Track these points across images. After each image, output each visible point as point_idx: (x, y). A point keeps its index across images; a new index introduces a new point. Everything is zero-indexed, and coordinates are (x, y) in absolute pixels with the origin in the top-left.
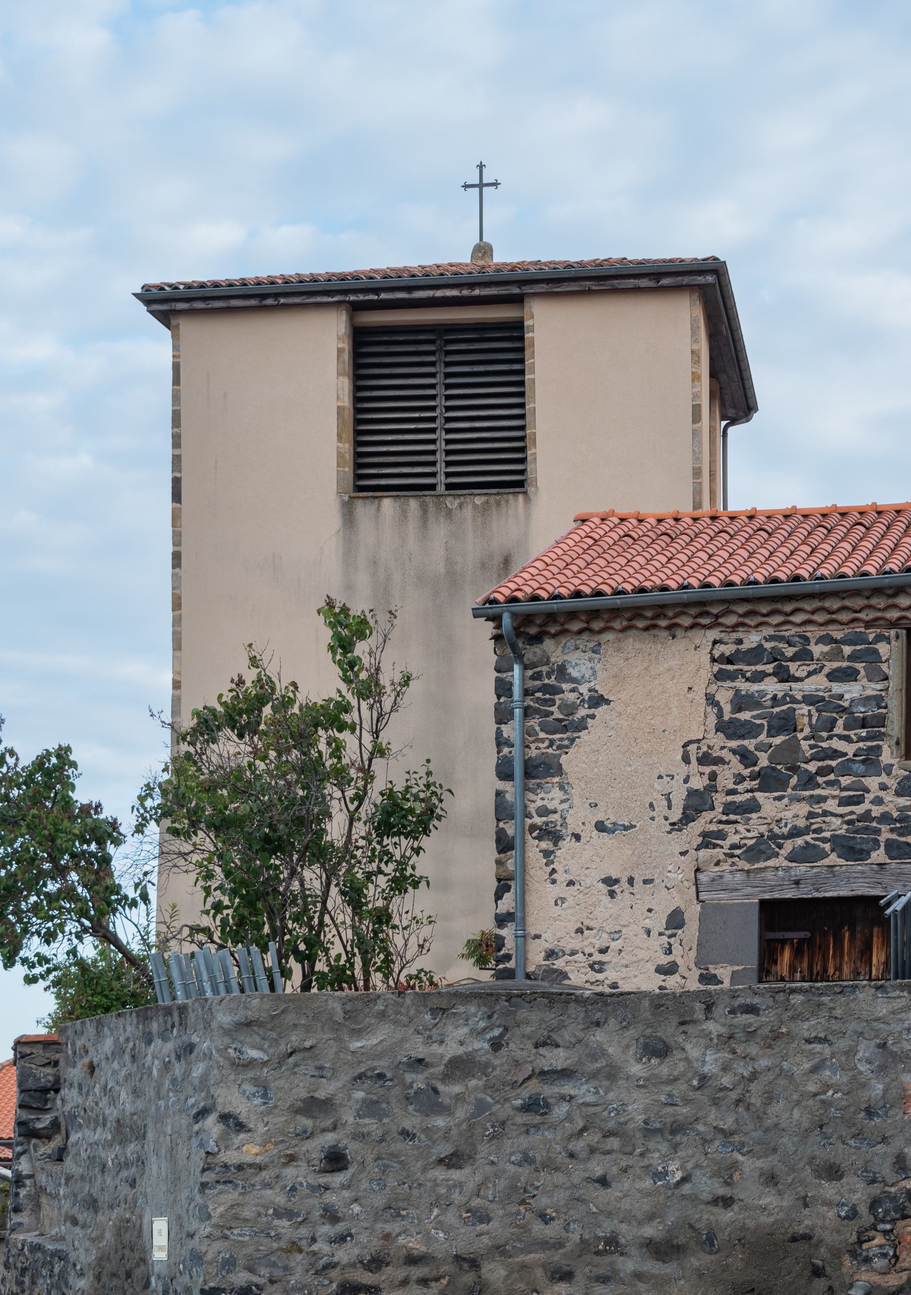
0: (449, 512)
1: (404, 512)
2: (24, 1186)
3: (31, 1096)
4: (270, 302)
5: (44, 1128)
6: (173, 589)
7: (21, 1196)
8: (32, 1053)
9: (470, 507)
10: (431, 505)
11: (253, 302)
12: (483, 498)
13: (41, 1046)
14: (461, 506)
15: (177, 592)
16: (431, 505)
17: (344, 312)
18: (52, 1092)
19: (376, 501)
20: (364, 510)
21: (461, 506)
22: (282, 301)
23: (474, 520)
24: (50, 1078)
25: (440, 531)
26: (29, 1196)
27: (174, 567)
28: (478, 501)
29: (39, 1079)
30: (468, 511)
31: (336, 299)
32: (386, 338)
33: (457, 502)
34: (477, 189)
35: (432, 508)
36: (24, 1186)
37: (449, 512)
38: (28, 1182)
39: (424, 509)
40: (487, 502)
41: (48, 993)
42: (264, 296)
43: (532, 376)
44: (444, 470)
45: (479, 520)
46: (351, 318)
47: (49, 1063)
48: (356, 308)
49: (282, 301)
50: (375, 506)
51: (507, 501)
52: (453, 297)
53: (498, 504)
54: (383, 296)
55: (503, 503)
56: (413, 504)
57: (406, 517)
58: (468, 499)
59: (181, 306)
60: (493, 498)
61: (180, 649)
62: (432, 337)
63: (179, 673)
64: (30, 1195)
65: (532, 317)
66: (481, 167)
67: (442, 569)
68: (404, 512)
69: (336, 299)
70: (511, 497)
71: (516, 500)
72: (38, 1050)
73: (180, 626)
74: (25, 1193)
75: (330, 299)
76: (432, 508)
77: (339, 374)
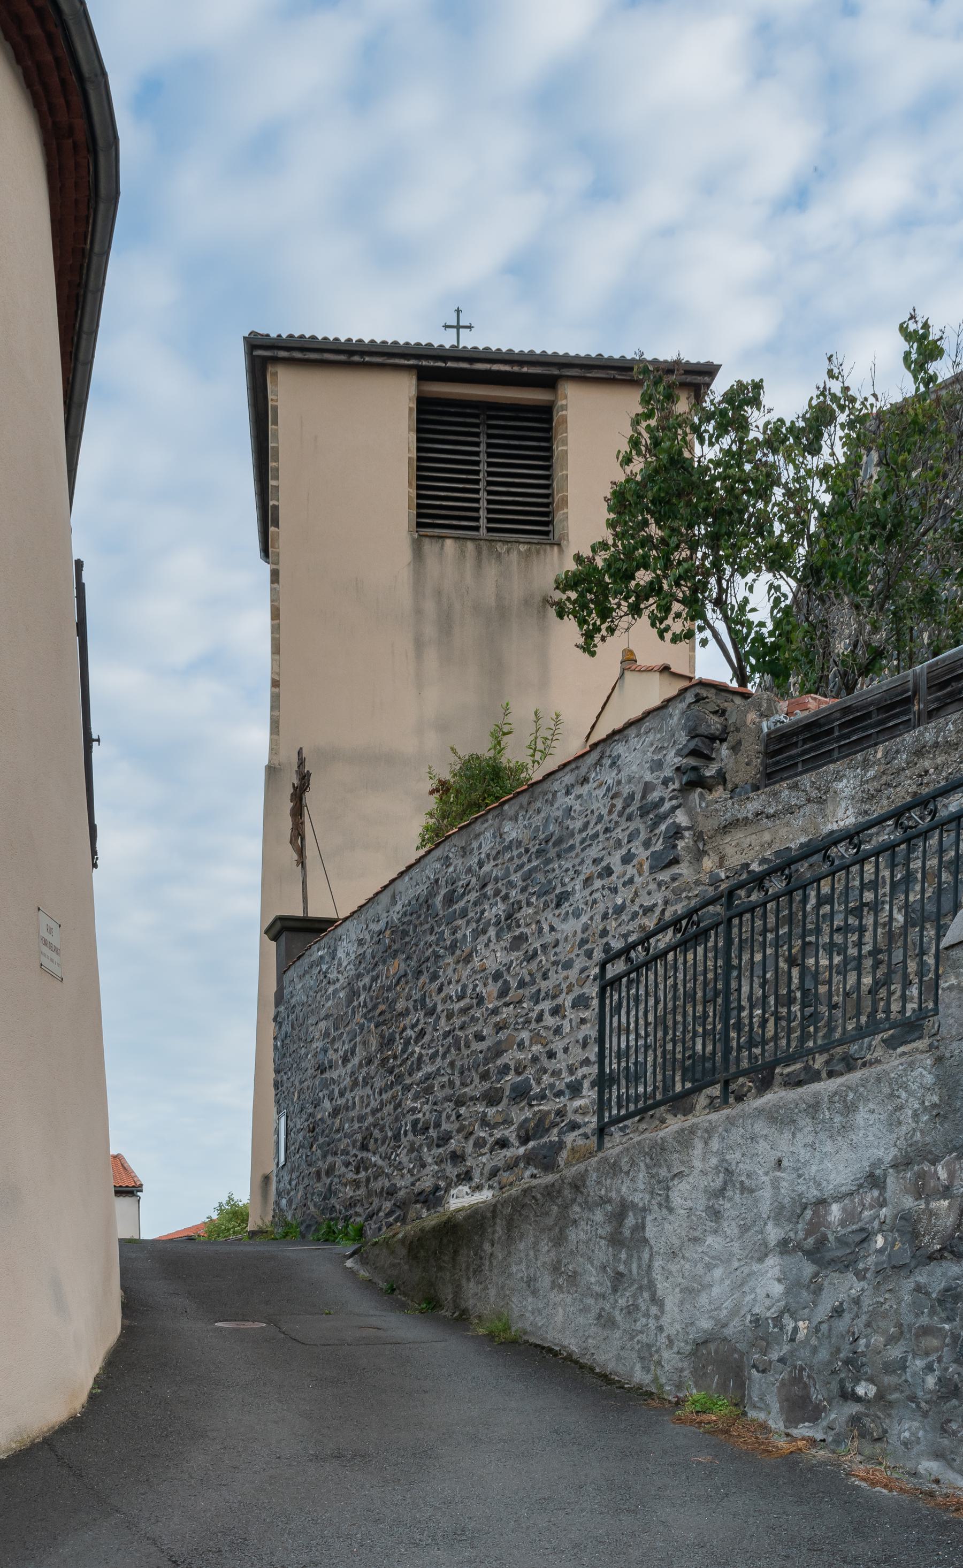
0: (499, 556)
1: (463, 552)
2: (682, 838)
3: (703, 742)
4: (356, 358)
5: (711, 777)
6: (272, 601)
7: (679, 848)
8: (707, 697)
9: (516, 552)
10: (484, 548)
11: (342, 357)
12: (526, 546)
13: (713, 691)
14: (508, 551)
15: (276, 604)
16: (484, 548)
17: (414, 377)
18: (718, 742)
19: (440, 541)
20: (429, 547)
21: (508, 551)
22: (367, 359)
23: (519, 564)
24: (719, 726)
25: (491, 571)
26: (687, 848)
27: (272, 582)
28: (522, 548)
29: (710, 726)
30: (514, 556)
31: (411, 362)
32: (440, 409)
33: (505, 547)
34: (461, 324)
35: (485, 552)
36: (682, 838)
37: (499, 556)
38: (687, 834)
39: (479, 551)
40: (529, 549)
41: (432, 797)
42: (352, 353)
43: (564, 448)
44: (485, 524)
45: (523, 564)
46: (418, 385)
47: (717, 711)
48: (424, 375)
49: (367, 359)
50: (439, 545)
51: (545, 551)
52: (506, 372)
53: (538, 552)
54: (450, 364)
55: (542, 552)
56: (470, 546)
57: (464, 557)
58: (515, 545)
59: (282, 354)
60: (534, 546)
61: (279, 653)
62: (476, 411)
63: (278, 674)
64: (688, 847)
65: (566, 398)
66: (458, 311)
67: (493, 604)
68: (463, 552)
69: (411, 362)
70: (548, 547)
71: (552, 550)
72: (711, 694)
73: (279, 633)
74: (683, 844)
75: (406, 362)
76: (485, 552)
77: (410, 430)
